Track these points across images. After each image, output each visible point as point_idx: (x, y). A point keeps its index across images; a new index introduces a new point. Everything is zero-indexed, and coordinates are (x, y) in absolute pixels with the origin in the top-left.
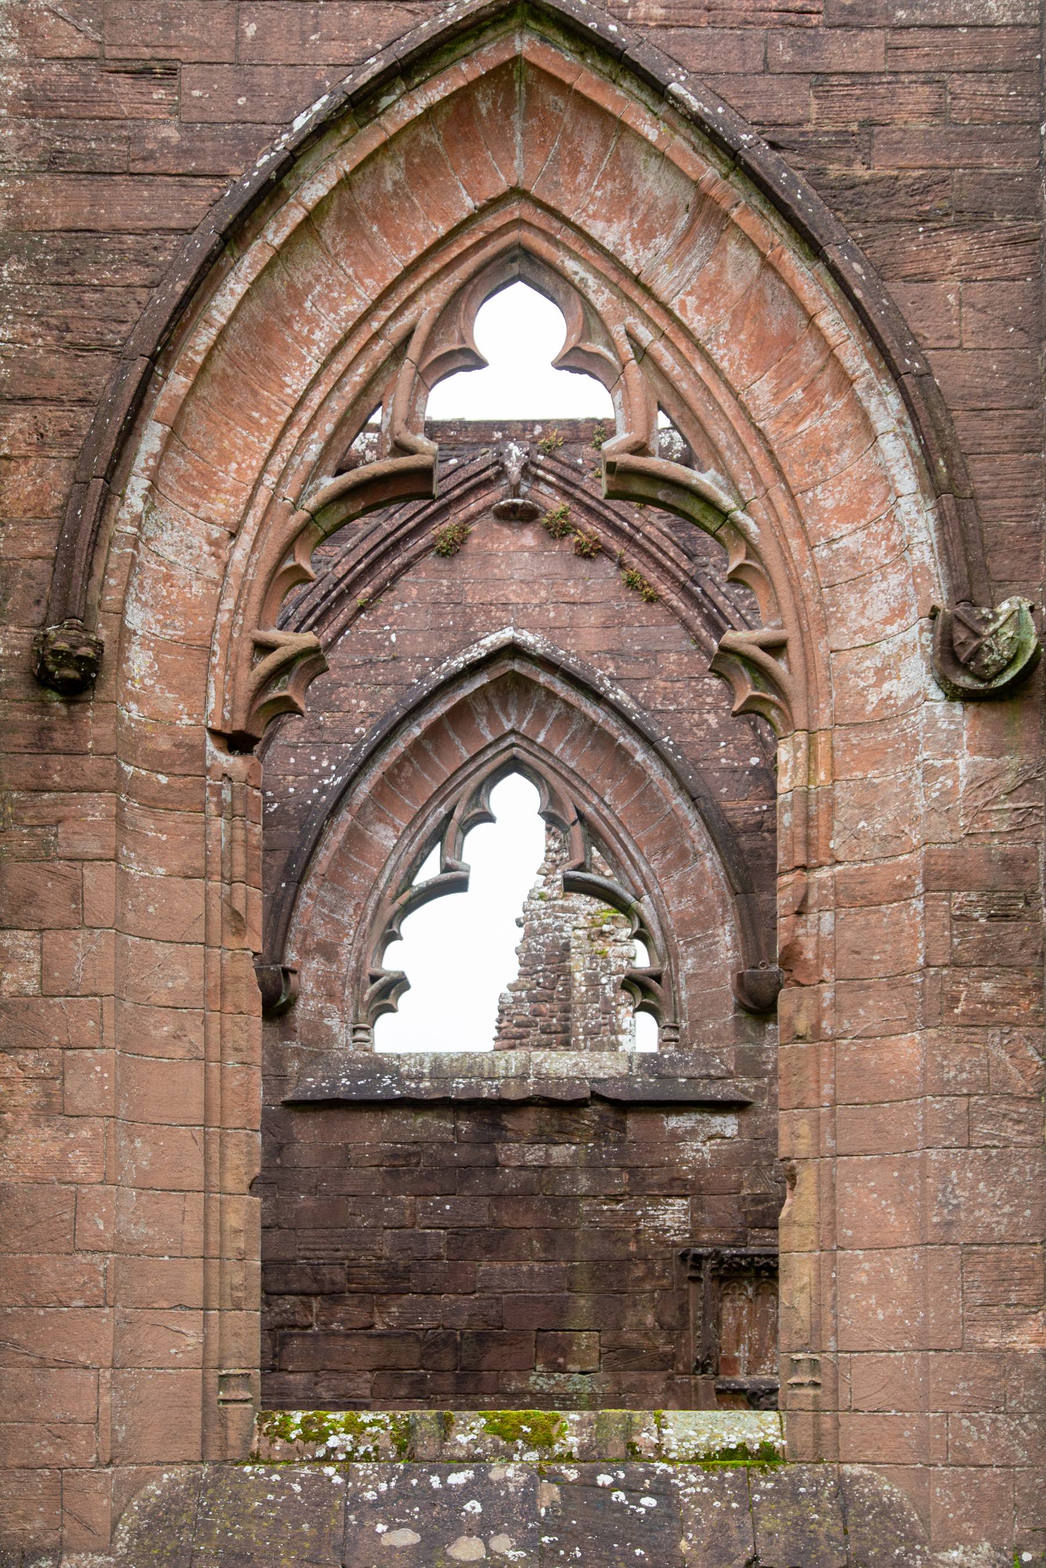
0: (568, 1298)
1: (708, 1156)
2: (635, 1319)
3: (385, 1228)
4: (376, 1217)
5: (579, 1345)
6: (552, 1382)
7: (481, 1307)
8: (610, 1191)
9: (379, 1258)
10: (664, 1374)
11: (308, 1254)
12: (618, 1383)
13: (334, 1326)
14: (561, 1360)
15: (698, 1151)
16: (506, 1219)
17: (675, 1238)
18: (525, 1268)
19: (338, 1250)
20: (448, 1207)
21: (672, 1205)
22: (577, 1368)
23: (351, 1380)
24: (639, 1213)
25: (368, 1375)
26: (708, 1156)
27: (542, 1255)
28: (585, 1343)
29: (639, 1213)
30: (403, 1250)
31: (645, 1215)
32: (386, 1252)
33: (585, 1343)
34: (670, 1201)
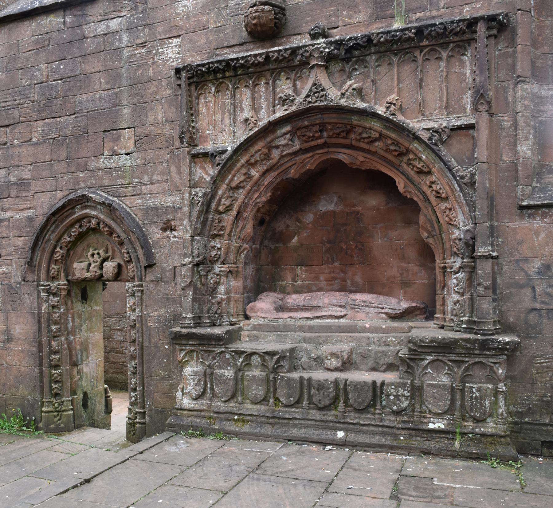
0: (118, 110)
1: (190, 8)
2: (153, 117)
3: (35, 84)
4: (31, 79)
5: (124, 137)
6: (112, 161)
7: (78, 122)
8: (139, 41)
9: (33, 102)
10: (168, 150)
11: (4, 104)
12: (144, 159)
13: (15, 142)
14: (116, 148)
15: (185, 6)
16: (88, 68)
17: (173, 64)
18: (97, 96)
19: (16, 100)
20: (62, 67)
21: (172, 43)
22: (123, 152)
23: (23, 170)
24: (154, 52)
25: (30, 167)
26: (190, 8)
27: (105, 87)
28: (127, 136)
29: (154, 52)
30: (42, 95)
31: (157, 53)
32: (36, 98)
33: (127, 136)
34: (171, 41)
